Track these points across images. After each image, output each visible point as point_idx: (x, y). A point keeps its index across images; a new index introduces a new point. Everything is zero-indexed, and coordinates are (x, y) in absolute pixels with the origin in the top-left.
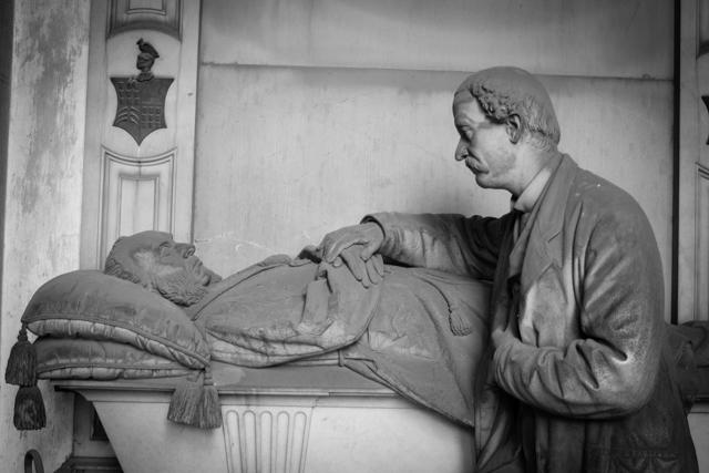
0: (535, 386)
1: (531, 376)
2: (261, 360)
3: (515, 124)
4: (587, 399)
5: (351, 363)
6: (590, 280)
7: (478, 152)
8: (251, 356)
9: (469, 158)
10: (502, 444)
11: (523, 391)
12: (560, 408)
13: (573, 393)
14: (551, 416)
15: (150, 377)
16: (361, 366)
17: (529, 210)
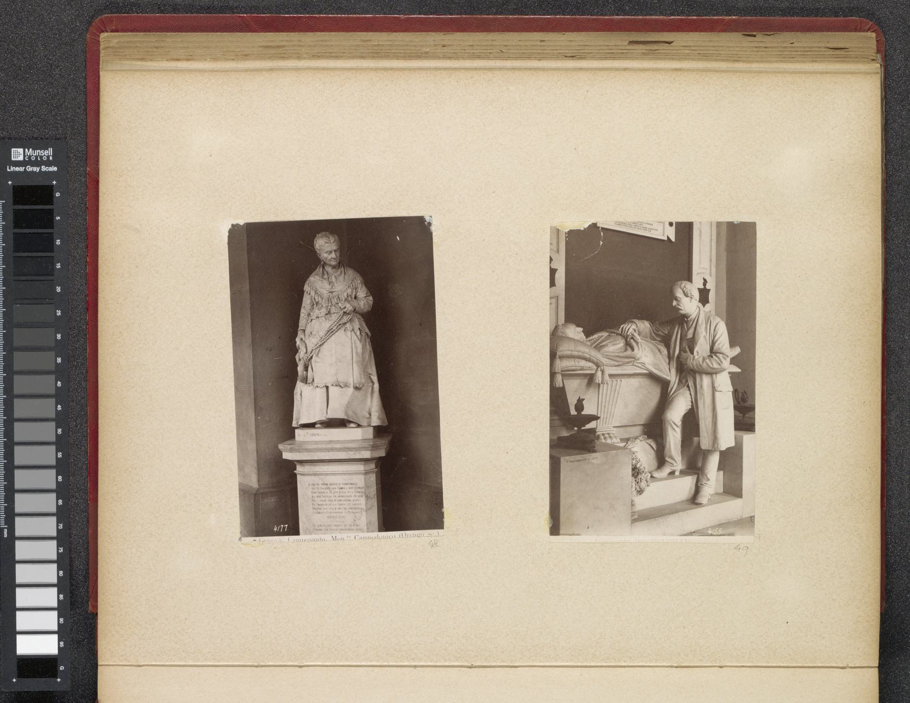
0: (704, 365)
1: (703, 363)
2: (617, 363)
3: (691, 298)
4: (719, 367)
5: (637, 364)
6: (716, 338)
7: (681, 304)
8: (613, 363)
9: (678, 306)
10: (678, 384)
11: (699, 366)
12: (710, 370)
13: (716, 366)
14: (702, 372)
15: (587, 369)
16: (639, 365)
17: (691, 320)
